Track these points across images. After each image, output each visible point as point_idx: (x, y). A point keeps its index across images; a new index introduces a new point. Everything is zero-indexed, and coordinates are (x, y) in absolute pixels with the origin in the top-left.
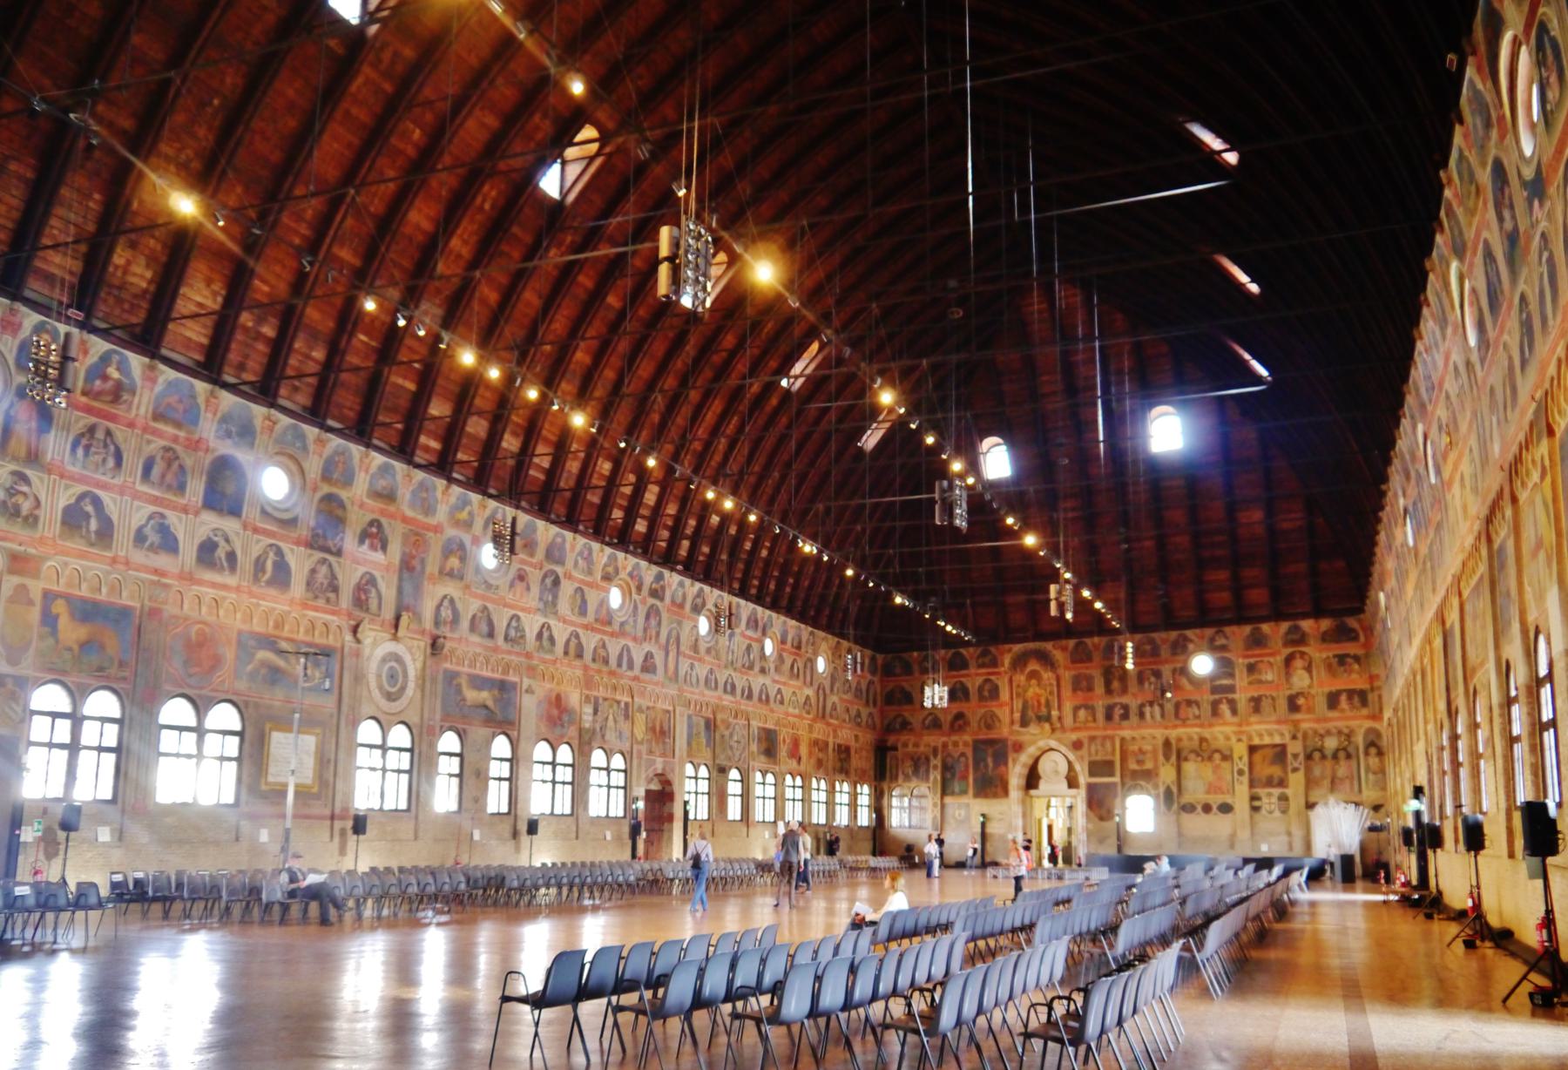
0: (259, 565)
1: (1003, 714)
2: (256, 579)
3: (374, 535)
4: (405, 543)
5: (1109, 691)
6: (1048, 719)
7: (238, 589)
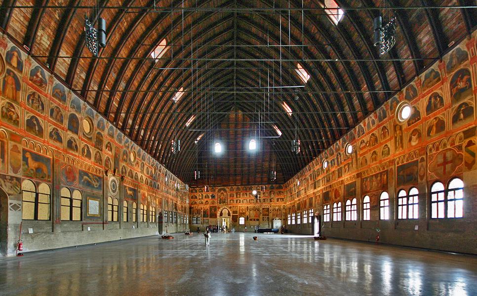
0: (83, 149)
1: (216, 201)
2: (83, 155)
3: (109, 146)
4: (115, 150)
5: (237, 197)
6: (225, 202)
7: (79, 157)
